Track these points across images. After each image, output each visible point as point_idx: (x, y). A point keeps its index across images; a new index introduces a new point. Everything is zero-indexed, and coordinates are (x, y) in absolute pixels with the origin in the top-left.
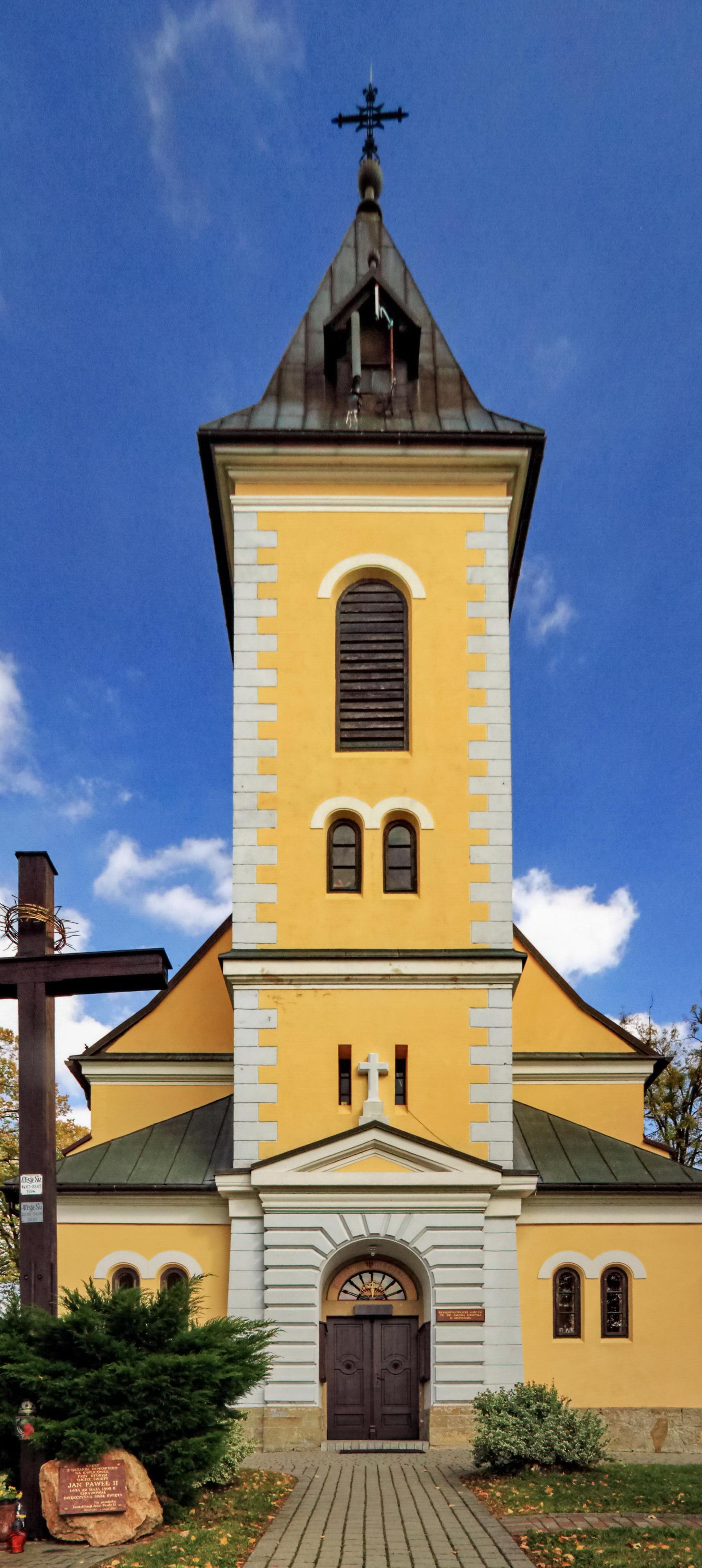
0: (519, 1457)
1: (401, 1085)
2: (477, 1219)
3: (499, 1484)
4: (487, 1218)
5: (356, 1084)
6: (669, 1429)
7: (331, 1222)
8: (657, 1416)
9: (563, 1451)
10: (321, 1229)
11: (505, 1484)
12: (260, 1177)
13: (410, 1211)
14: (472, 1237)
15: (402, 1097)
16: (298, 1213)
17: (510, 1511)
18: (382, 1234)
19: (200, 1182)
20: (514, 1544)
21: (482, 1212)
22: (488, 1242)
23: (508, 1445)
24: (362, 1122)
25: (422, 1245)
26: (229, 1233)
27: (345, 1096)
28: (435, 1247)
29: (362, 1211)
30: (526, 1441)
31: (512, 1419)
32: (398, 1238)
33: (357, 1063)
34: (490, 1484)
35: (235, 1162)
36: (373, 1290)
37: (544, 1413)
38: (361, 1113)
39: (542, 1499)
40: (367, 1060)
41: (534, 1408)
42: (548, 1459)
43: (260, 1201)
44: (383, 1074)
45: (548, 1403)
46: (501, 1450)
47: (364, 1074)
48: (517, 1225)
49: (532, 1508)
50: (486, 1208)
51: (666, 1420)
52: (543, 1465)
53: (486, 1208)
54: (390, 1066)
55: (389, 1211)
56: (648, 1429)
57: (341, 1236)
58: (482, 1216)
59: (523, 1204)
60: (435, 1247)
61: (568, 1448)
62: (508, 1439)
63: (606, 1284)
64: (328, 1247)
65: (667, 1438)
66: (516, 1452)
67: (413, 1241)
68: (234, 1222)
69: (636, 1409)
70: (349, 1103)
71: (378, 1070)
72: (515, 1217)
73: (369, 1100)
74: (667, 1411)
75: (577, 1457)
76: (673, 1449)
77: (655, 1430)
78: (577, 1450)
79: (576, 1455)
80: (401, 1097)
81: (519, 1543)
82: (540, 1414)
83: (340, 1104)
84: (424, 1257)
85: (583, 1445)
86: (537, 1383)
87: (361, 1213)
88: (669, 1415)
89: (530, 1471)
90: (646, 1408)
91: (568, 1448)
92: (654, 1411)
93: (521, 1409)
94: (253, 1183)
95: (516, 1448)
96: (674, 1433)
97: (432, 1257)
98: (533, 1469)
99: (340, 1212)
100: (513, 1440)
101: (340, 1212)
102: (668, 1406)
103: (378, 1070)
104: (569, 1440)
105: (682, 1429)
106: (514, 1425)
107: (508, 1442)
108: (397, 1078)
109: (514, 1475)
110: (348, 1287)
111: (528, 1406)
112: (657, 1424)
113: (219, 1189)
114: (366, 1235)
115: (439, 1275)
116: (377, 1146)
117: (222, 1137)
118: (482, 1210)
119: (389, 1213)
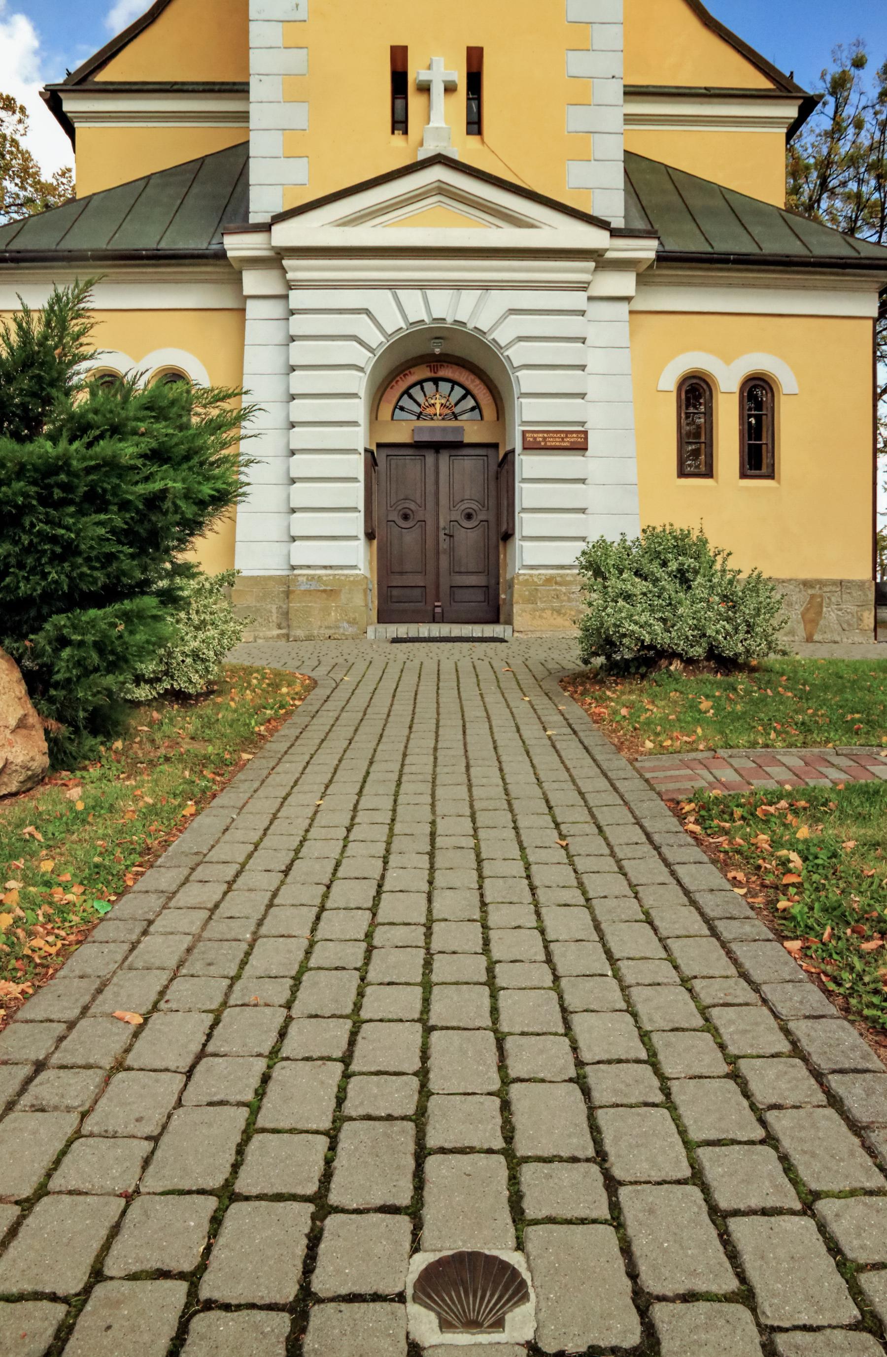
0: (651, 647)
1: (475, 110)
2: (577, 300)
3: (623, 693)
4: (590, 299)
5: (415, 101)
6: (824, 609)
8: (810, 592)
9: (720, 637)
10: (367, 312)
11: (631, 692)
13: (486, 287)
14: (571, 326)
15: (476, 126)
16: (335, 288)
17: (649, 745)
18: (450, 320)
19: (204, 246)
20: (673, 822)
21: (585, 289)
22: (591, 332)
23: (636, 628)
24: (422, 156)
25: (502, 336)
26: (243, 320)
27: (400, 123)
28: (521, 339)
29: (422, 286)
30: (664, 620)
31: (641, 586)
32: (471, 326)
33: (416, 73)
34: (608, 693)
35: (251, 215)
36: (438, 406)
37: (690, 575)
38: (421, 144)
39: (698, 721)
40: (429, 67)
41: (673, 566)
42: (698, 651)
43: (284, 271)
44: (450, 89)
45: (697, 558)
46: (624, 635)
47: (425, 89)
48: (631, 312)
49: (685, 738)
50: (589, 283)
51: (821, 596)
52: (689, 662)
53: (589, 283)
54: (460, 78)
55: (459, 286)
56: (799, 609)
57: (394, 322)
58: (583, 295)
59: (638, 283)
60: (521, 339)
61: (727, 633)
62: (636, 617)
63: (746, 400)
64: (375, 338)
65: (822, 622)
66: (647, 639)
67: (493, 328)
68: (250, 305)
69: (783, 582)
70: (405, 132)
71: (444, 82)
72: (628, 299)
73: (431, 125)
74: (822, 583)
75: (740, 649)
76: (828, 636)
77: (807, 610)
78: (741, 636)
79: (740, 645)
80: (475, 125)
81: (682, 818)
82: (683, 578)
83: (393, 133)
84: (506, 354)
85: (750, 629)
86: (677, 526)
87: (421, 288)
88: (825, 589)
89: (668, 670)
90: (796, 580)
91: (727, 633)
92: (807, 584)
93: (655, 568)
94: (274, 243)
95: (648, 633)
96: (831, 615)
97: (517, 355)
98: (672, 668)
99: (392, 286)
100: (643, 619)
101: (392, 286)
102: (824, 576)
103: (444, 82)
104: (728, 620)
105: (840, 610)
106: (644, 594)
107: (636, 623)
108: (468, 99)
109: (643, 677)
110: (406, 402)
111: (664, 564)
112: (809, 603)
113: (230, 254)
114: (427, 320)
115: (526, 381)
116: (442, 190)
117: (239, 189)
118: (583, 287)
119: (459, 288)
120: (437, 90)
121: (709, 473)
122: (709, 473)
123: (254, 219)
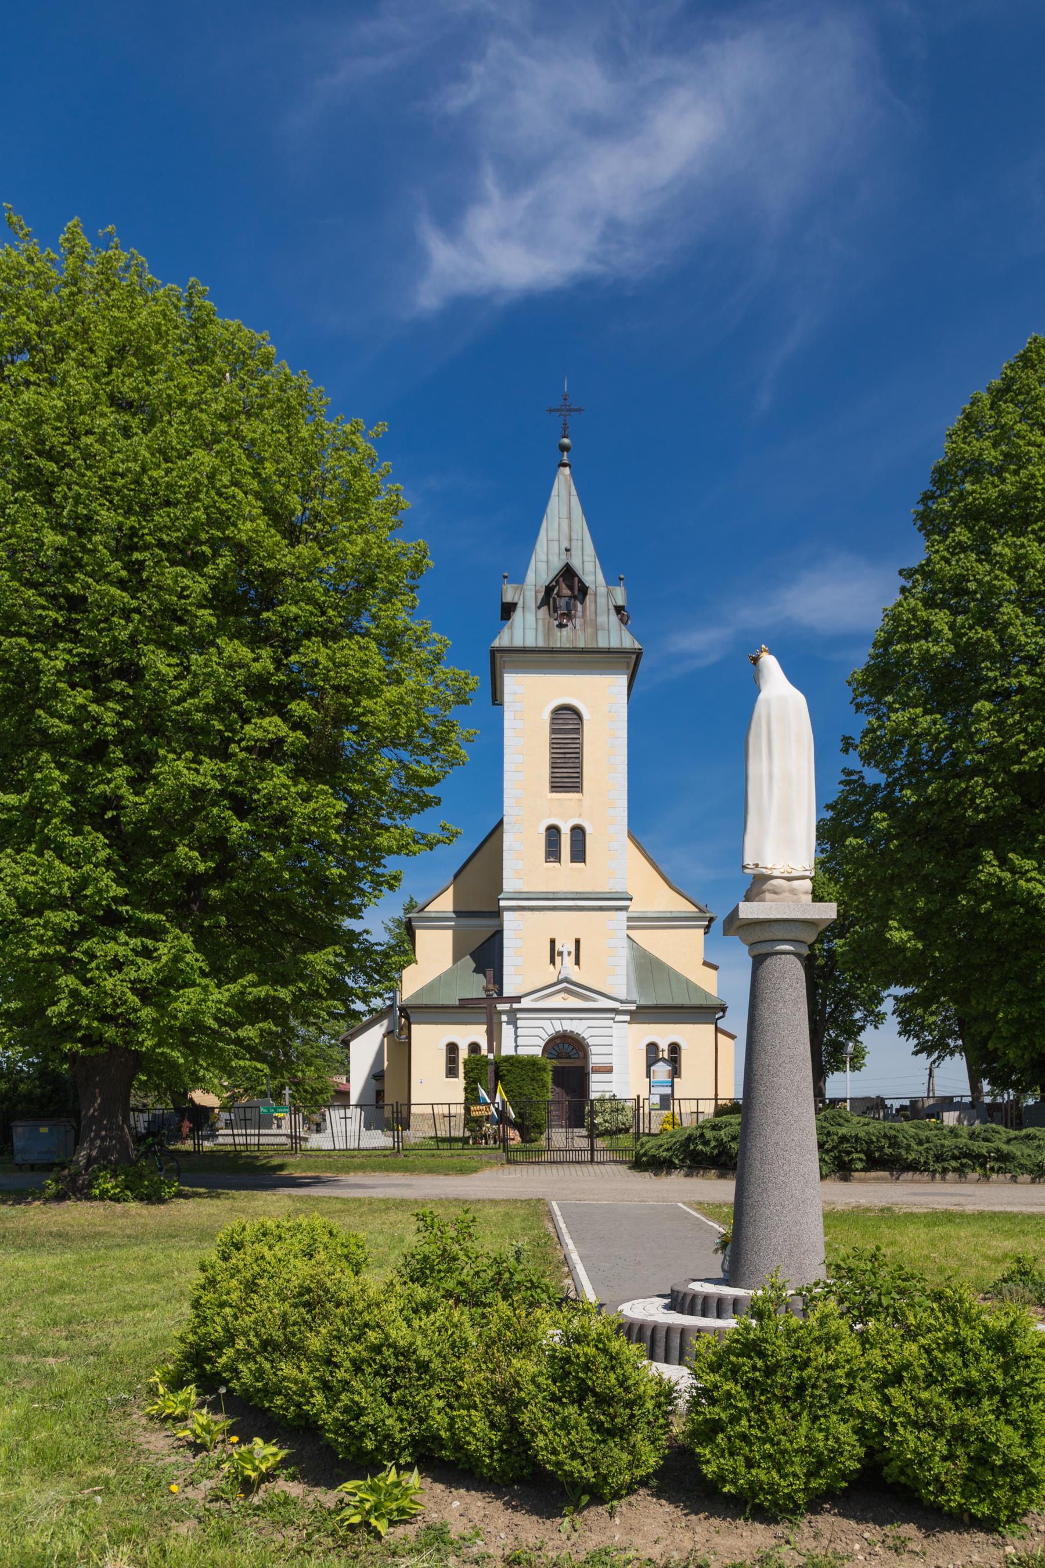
2: (610, 1023)
5: (558, 959)
7: (546, 1024)
14: (607, 1031)
25: (585, 1035)
27: (553, 961)
44: (569, 953)
47: (561, 954)
54: (573, 950)
57: (551, 1031)
80: (577, 962)
97: (590, 1041)
115: (593, 1050)
116: (565, 990)
120: (565, 954)
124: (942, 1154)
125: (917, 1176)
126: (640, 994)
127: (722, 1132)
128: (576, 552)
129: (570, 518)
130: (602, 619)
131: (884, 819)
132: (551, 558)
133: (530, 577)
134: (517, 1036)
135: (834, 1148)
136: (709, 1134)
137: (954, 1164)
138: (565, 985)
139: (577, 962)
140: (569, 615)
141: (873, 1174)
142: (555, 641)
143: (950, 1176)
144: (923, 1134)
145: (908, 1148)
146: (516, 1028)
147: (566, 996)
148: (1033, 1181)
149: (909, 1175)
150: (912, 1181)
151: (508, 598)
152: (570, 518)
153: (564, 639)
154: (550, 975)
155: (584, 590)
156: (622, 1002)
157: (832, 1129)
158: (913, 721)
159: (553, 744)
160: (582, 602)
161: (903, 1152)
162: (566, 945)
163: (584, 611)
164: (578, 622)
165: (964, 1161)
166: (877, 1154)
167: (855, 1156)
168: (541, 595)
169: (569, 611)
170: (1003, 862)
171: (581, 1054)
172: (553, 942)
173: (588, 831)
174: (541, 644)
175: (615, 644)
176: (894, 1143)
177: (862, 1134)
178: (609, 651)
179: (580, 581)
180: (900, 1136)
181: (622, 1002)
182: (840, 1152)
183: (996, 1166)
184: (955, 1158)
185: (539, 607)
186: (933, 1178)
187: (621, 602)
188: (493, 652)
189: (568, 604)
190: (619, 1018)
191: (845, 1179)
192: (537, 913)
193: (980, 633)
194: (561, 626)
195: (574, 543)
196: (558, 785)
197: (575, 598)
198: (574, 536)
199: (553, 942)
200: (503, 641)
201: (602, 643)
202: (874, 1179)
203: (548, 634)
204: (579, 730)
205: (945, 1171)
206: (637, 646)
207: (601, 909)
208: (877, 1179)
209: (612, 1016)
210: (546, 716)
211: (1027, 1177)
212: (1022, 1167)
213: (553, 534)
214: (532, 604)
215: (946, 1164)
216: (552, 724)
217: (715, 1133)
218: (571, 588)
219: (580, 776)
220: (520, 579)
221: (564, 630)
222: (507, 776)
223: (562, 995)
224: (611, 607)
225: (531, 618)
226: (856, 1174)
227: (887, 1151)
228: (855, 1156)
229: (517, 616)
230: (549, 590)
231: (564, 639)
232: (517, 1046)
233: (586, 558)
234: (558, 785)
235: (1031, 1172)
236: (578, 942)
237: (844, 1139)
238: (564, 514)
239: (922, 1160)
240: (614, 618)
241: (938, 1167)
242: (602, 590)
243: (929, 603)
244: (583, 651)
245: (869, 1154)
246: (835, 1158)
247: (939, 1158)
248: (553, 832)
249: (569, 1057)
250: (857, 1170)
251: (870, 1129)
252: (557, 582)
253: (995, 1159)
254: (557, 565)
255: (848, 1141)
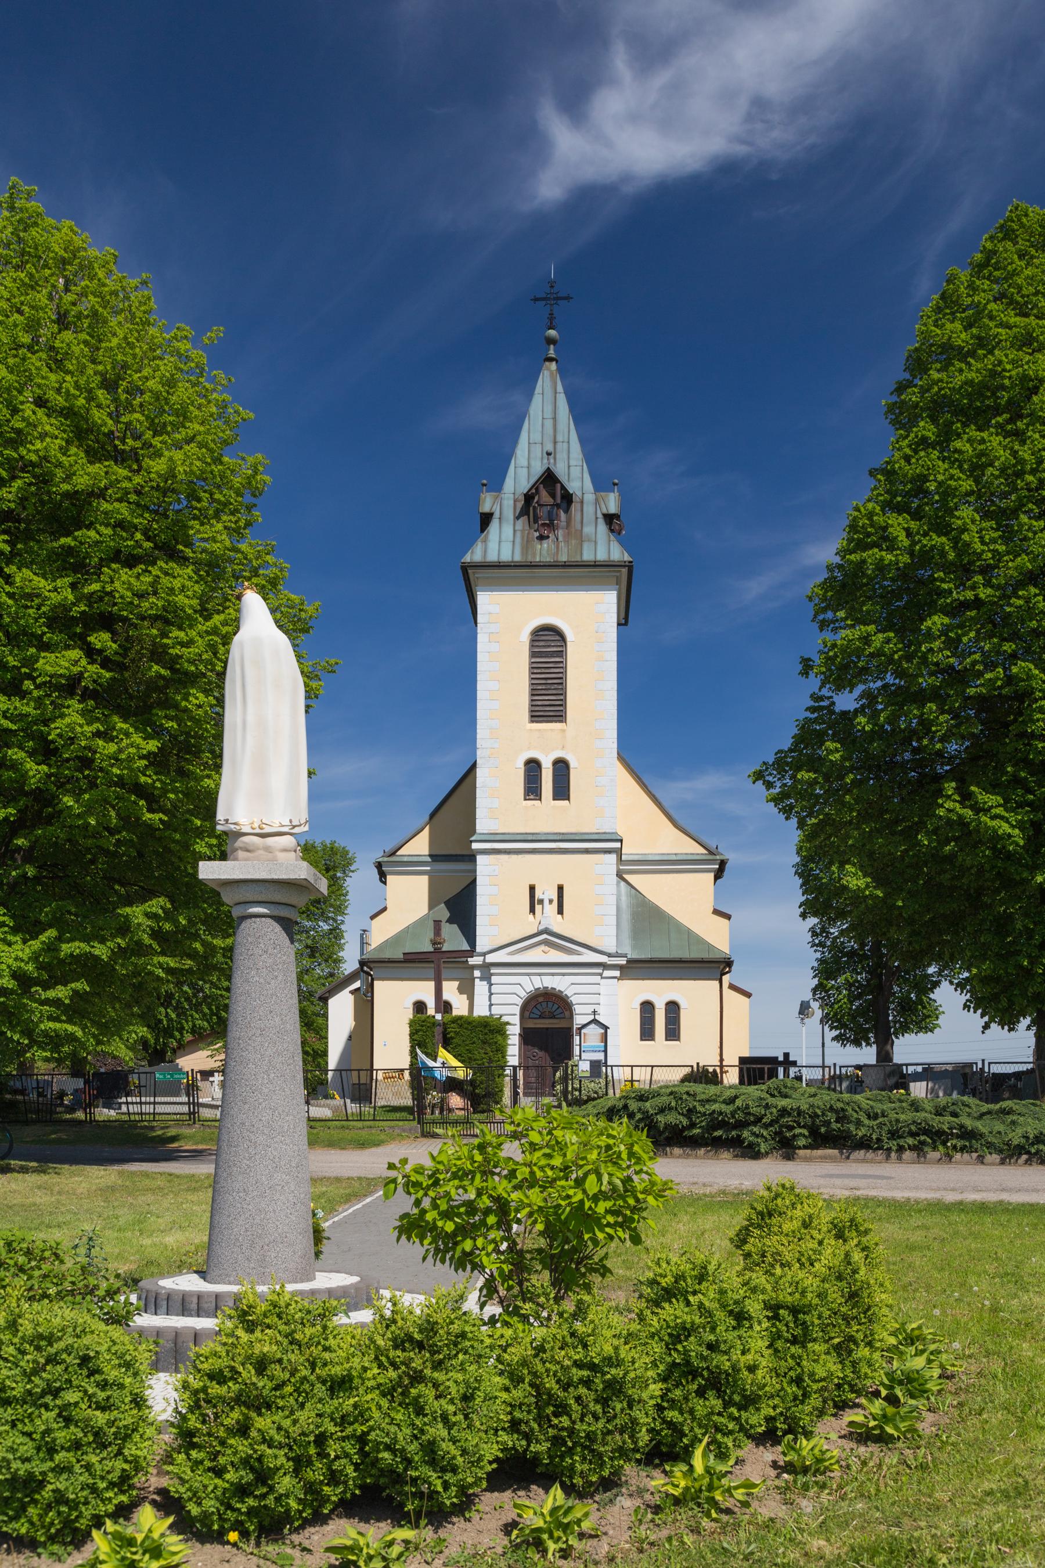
5: (538, 908)
7: (525, 980)
12: (491, 958)
13: (564, 975)
22: (602, 989)
25: (569, 993)
27: (532, 910)
29: (540, 975)
33: (538, 894)
44: (551, 901)
47: (541, 902)
55: (553, 974)
57: (530, 988)
64: (523, 994)
80: (560, 911)
97: (574, 1000)
116: (546, 942)
120: (546, 902)
121: (653, 1039)
122: (653, 1039)
123: (479, 949)
124: (897, 1131)
125: (870, 1155)
126: (634, 947)
127: (648, 1104)
128: (561, 456)
129: (555, 419)
130: (588, 530)
131: (837, 750)
132: (533, 463)
133: (509, 485)
134: (491, 994)
135: (771, 1124)
136: (633, 1106)
137: (910, 1141)
138: (545, 936)
139: (560, 911)
140: (551, 526)
141: (820, 1152)
142: (534, 555)
143: (908, 1155)
144: (878, 1108)
145: (859, 1123)
146: (491, 985)
147: (547, 948)
148: (1002, 1162)
149: (861, 1154)
150: (864, 1161)
151: (486, 508)
152: (555, 419)
153: (544, 552)
154: (529, 925)
155: (568, 498)
156: (610, 955)
157: (771, 1100)
158: (866, 640)
159: (533, 669)
160: (567, 510)
161: (852, 1128)
162: (547, 892)
163: (569, 522)
164: (560, 533)
165: (922, 1138)
166: (823, 1130)
167: (797, 1131)
168: (520, 505)
169: (551, 520)
170: (966, 797)
171: (567, 1014)
172: (532, 889)
173: (572, 765)
174: (518, 558)
175: (601, 556)
176: (842, 1117)
177: (804, 1107)
178: (595, 565)
179: (563, 487)
180: (850, 1109)
181: (610, 955)
182: (781, 1126)
183: (959, 1143)
184: (913, 1135)
185: (518, 518)
186: (888, 1157)
187: (613, 508)
188: (465, 569)
189: (550, 513)
190: (607, 973)
191: (789, 1157)
192: (514, 857)
193: (938, 540)
194: (541, 538)
195: (559, 446)
196: (537, 715)
197: (558, 506)
198: (560, 438)
199: (532, 889)
200: (475, 555)
201: (587, 556)
202: (821, 1157)
203: (526, 547)
204: (562, 654)
205: (901, 1149)
206: (627, 558)
207: (587, 851)
208: (824, 1158)
209: (600, 971)
210: (525, 637)
211: (996, 1157)
212: (990, 1146)
213: (536, 437)
214: (509, 513)
215: (901, 1142)
216: (532, 646)
217: (640, 1104)
218: (553, 495)
219: (563, 704)
220: (496, 486)
221: (545, 544)
222: (480, 705)
223: (543, 947)
224: (600, 515)
225: (508, 530)
226: (801, 1152)
227: (835, 1126)
228: (797, 1131)
229: (494, 526)
230: (528, 498)
231: (544, 552)
232: (491, 1005)
233: (572, 463)
234: (537, 715)
235: (1000, 1151)
236: (560, 889)
237: (784, 1112)
238: (549, 414)
239: (874, 1137)
240: (602, 527)
241: (893, 1144)
242: (590, 497)
243: (889, 506)
244: (565, 565)
245: (814, 1132)
246: (776, 1133)
247: (894, 1134)
248: (533, 767)
249: (554, 1017)
250: (800, 1148)
251: (816, 1101)
252: (537, 489)
253: (958, 1137)
254: (538, 469)
255: (789, 1114)
